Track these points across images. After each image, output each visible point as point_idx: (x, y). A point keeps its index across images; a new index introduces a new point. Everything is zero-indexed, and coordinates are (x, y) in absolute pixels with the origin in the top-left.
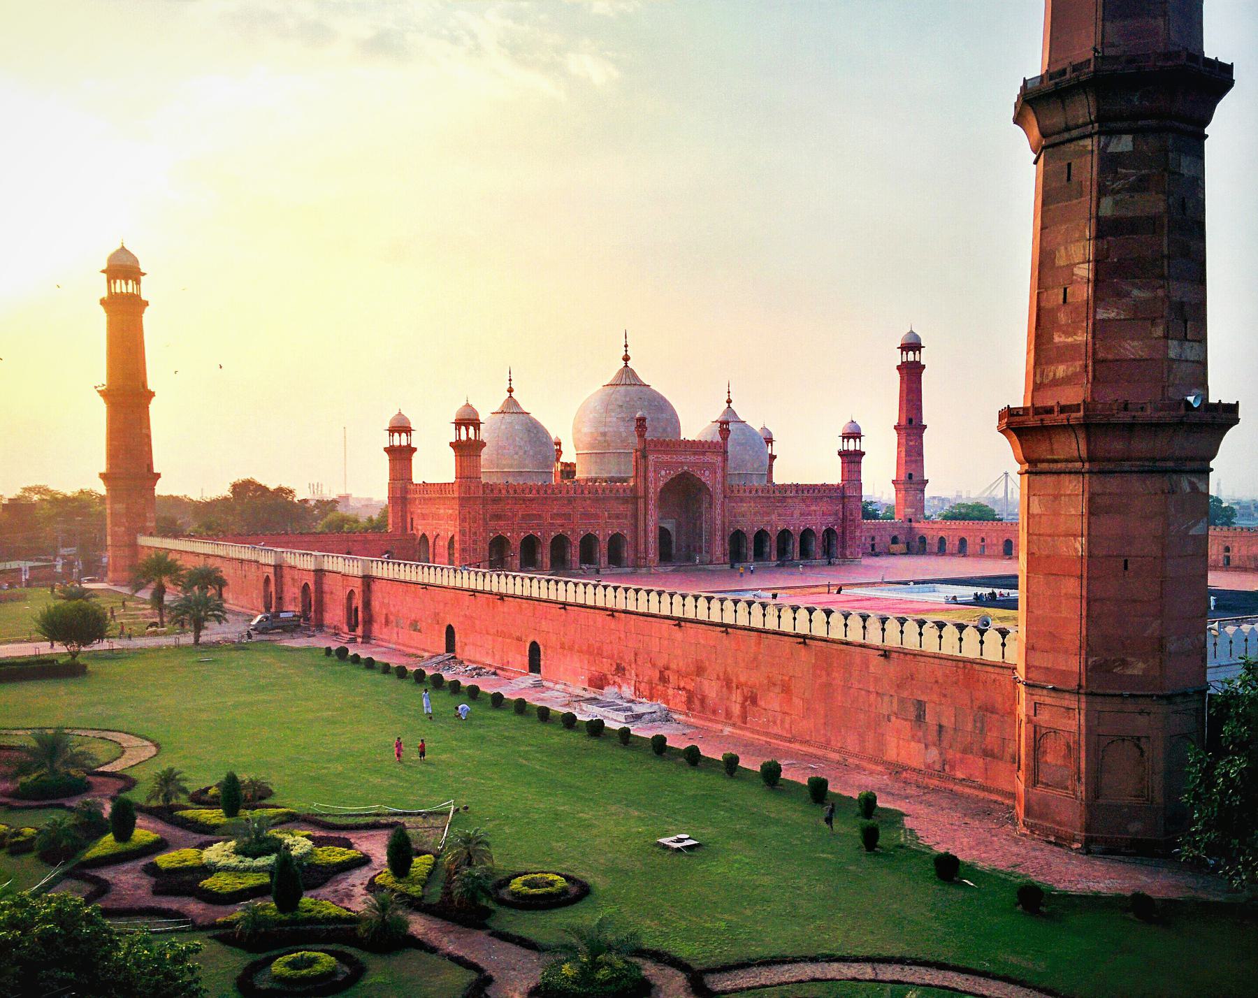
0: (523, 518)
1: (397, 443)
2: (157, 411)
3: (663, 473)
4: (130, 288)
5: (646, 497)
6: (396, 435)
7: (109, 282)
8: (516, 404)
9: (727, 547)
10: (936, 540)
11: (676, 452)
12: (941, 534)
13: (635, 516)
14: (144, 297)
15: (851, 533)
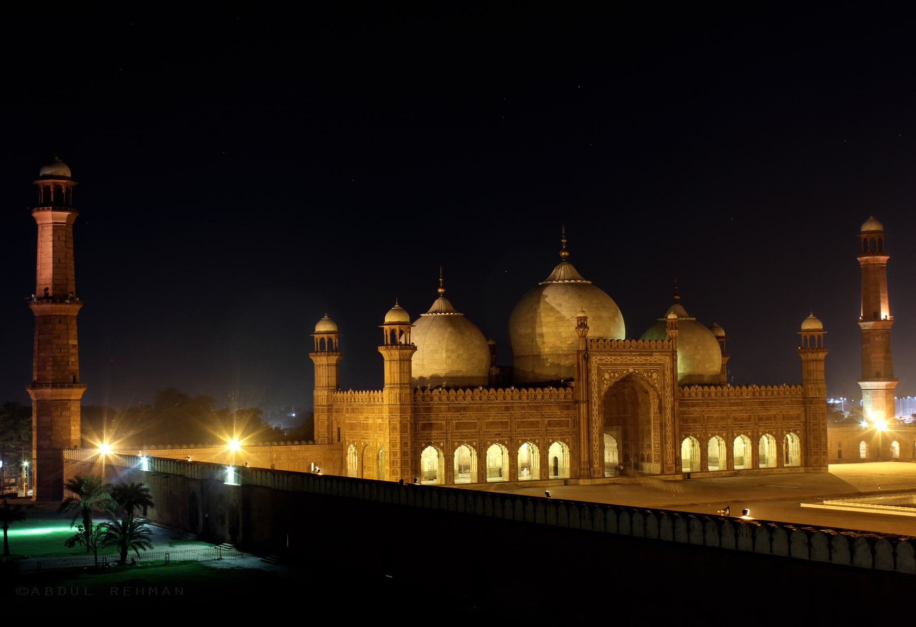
0: (458, 426)
3: (607, 376)
5: (588, 402)
13: (577, 423)
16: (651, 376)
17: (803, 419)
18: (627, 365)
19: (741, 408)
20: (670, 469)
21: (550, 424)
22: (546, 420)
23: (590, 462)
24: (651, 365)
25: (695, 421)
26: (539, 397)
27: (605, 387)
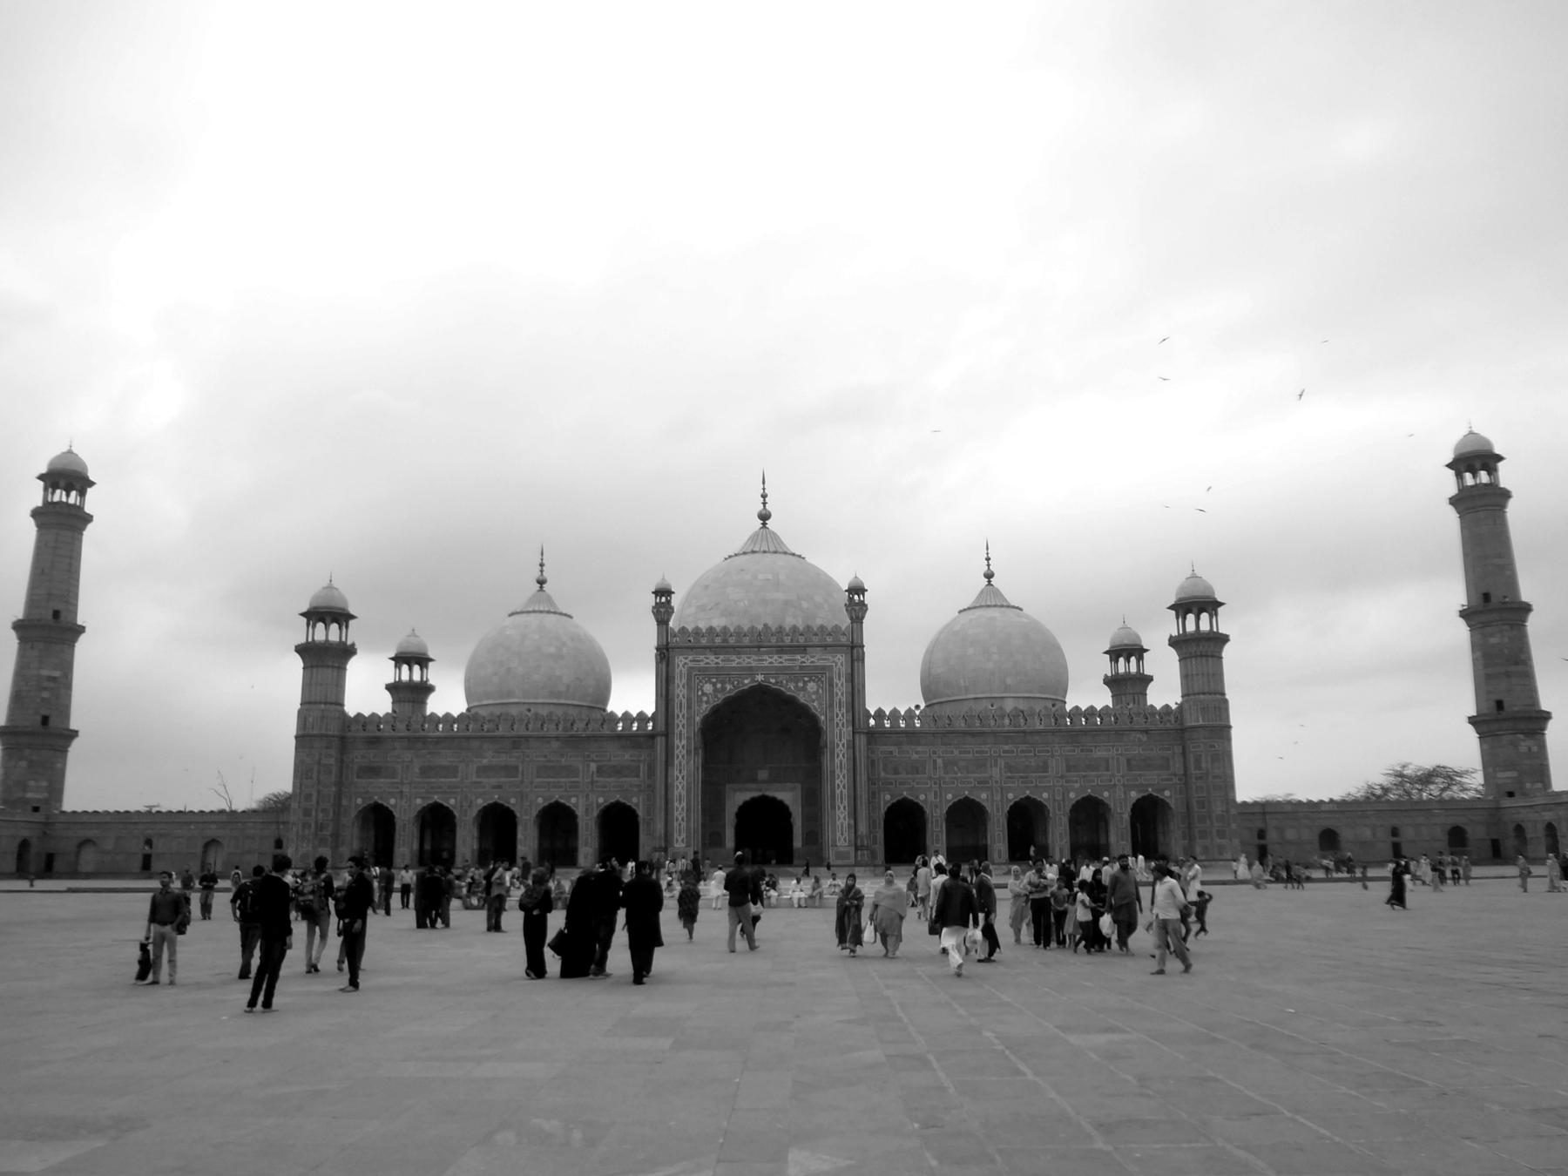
0: (426, 771)
1: (405, 677)
2: (84, 650)
3: (708, 688)
4: (73, 498)
5: (667, 733)
6: (405, 668)
7: (46, 490)
8: (549, 600)
9: (863, 828)
10: (1541, 832)
11: (737, 650)
12: (1548, 816)
13: (651, 772)
14: (87, 510)
15: (1202, 804)
16: (804, 689)
17: (1177, 766)
18: (751, 668)
19: (1023, 747)
20: (839, 855)
21: (600, 771)
22: (593, 766)
23: (668, 836)
24: (801, 668)
25: (916, 769)
26: (581, 725)
27: (705, 708)
